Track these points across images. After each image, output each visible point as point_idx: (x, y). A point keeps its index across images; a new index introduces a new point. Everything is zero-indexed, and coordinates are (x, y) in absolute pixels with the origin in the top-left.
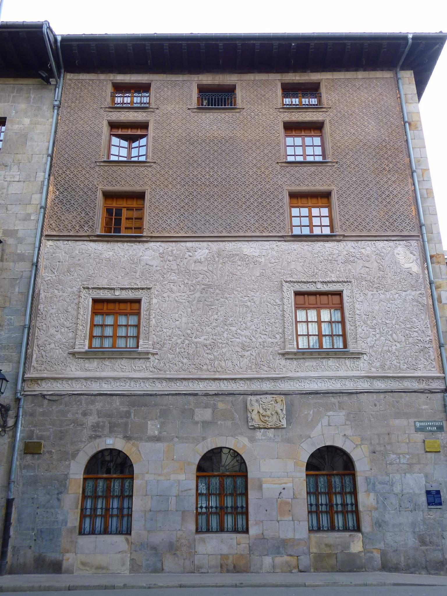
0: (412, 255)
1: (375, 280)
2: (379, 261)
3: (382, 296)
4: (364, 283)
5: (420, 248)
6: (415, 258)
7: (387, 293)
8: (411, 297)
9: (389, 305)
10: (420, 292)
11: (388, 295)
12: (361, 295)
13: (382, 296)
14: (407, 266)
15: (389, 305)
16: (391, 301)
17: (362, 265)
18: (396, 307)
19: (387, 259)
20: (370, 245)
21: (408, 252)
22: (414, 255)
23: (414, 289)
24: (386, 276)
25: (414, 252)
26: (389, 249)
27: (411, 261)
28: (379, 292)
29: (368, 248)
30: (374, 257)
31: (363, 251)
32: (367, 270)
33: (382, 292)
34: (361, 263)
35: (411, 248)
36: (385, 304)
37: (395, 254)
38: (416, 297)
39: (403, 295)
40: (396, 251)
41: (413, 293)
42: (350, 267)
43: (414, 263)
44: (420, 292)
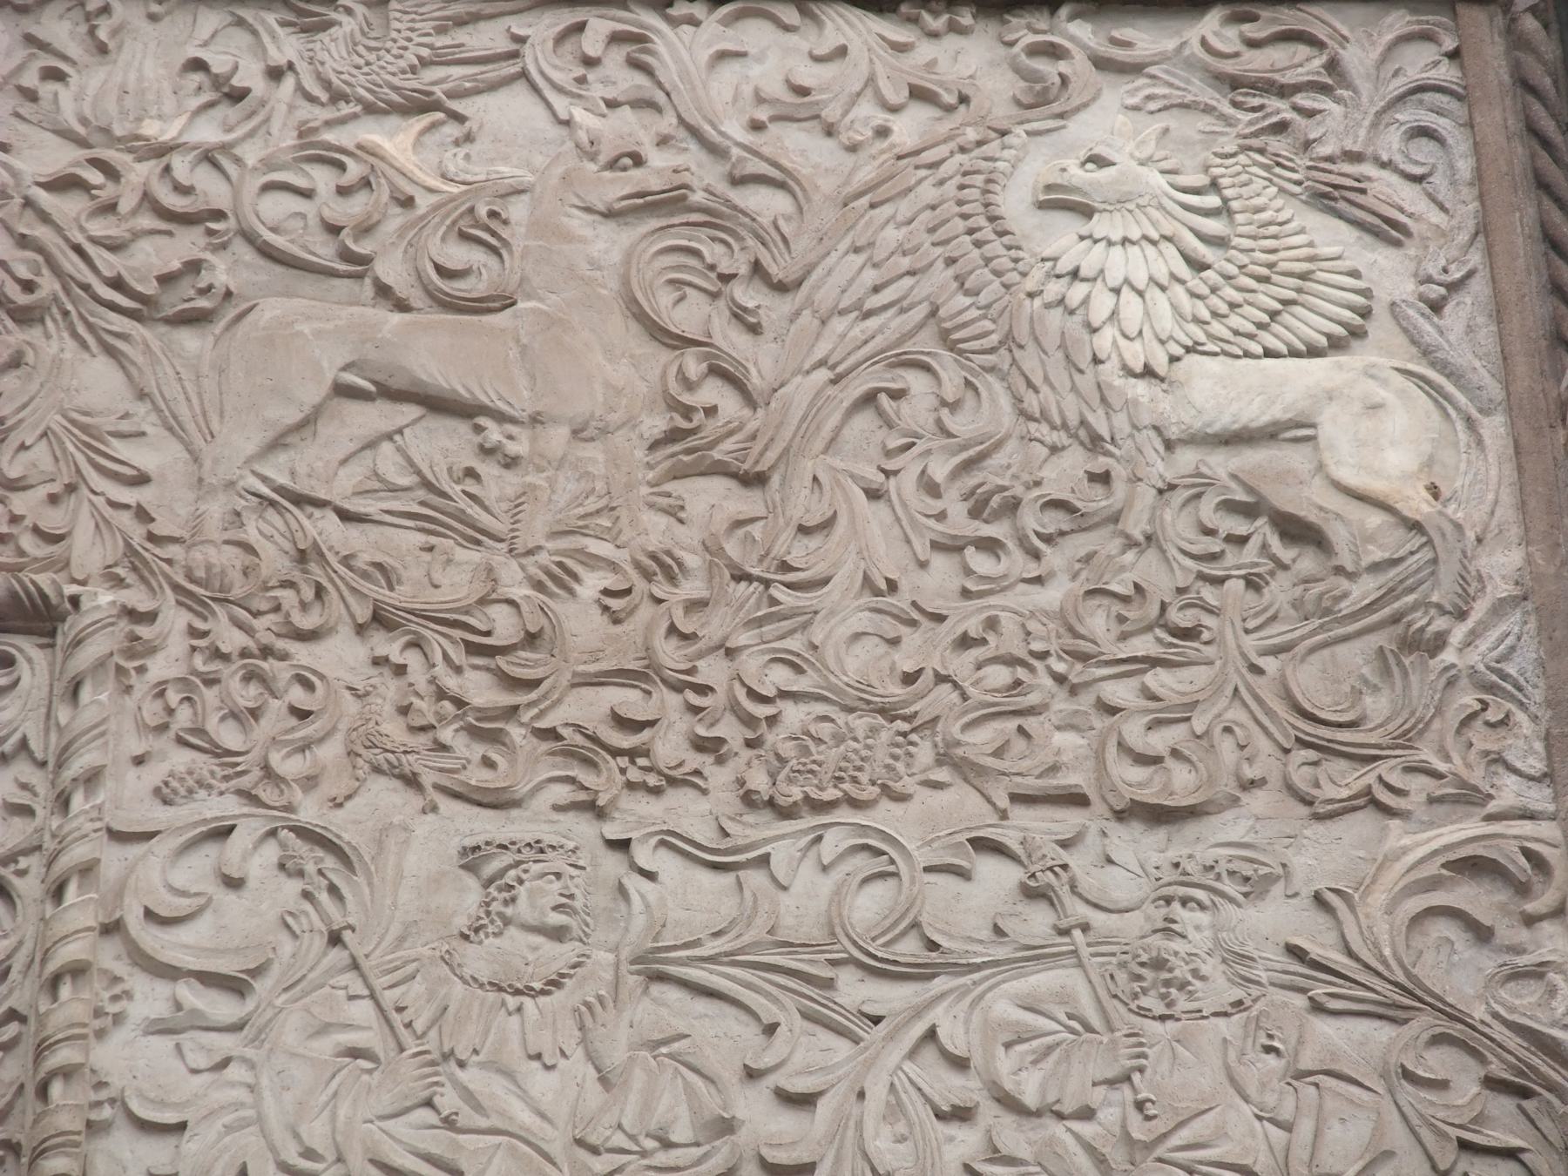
0: (1330, 236)
1: (580, 620)
2: (687, 316)
3: (687, 899)
4: (341, 657)
5: (1498, 117)
6: (1391, 274)
7: (784, 843)
8: (1274, 920)
9: (808, 1054)
10: (1461, 831)
11: (808, 886)
12: (260, 864)
13: (687, 899)
14: (1222, 390)
15: (808, 1054)
16: (854, 990)
17: (330, 363)
18: (953, 1087)
19: (842, 275)
20: (540, 57)
21: (1261, 194)
22: (1388, 230)
23: (1342, 780)
24: (799, 552)
25: (1388, 190)
26: (910, 126)
27: (1308, 325)
28: (637, 815)
29: (506, 113)
30: (607, 244)
31: (395, 141)
32: (440, 445)
33: (691, 814)
34: (319, 331)
35: (1334, 126)
36: (720, 1035)
37: (1015, 202)
38: (1378, 923)
39: (1121, 885)
40: (1034, 164)
41: (1323, 854)
42: (97, 384)
43: (1382, 351)
44: (1461, 831)
